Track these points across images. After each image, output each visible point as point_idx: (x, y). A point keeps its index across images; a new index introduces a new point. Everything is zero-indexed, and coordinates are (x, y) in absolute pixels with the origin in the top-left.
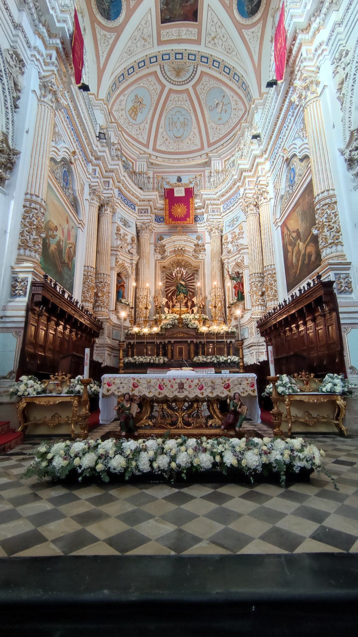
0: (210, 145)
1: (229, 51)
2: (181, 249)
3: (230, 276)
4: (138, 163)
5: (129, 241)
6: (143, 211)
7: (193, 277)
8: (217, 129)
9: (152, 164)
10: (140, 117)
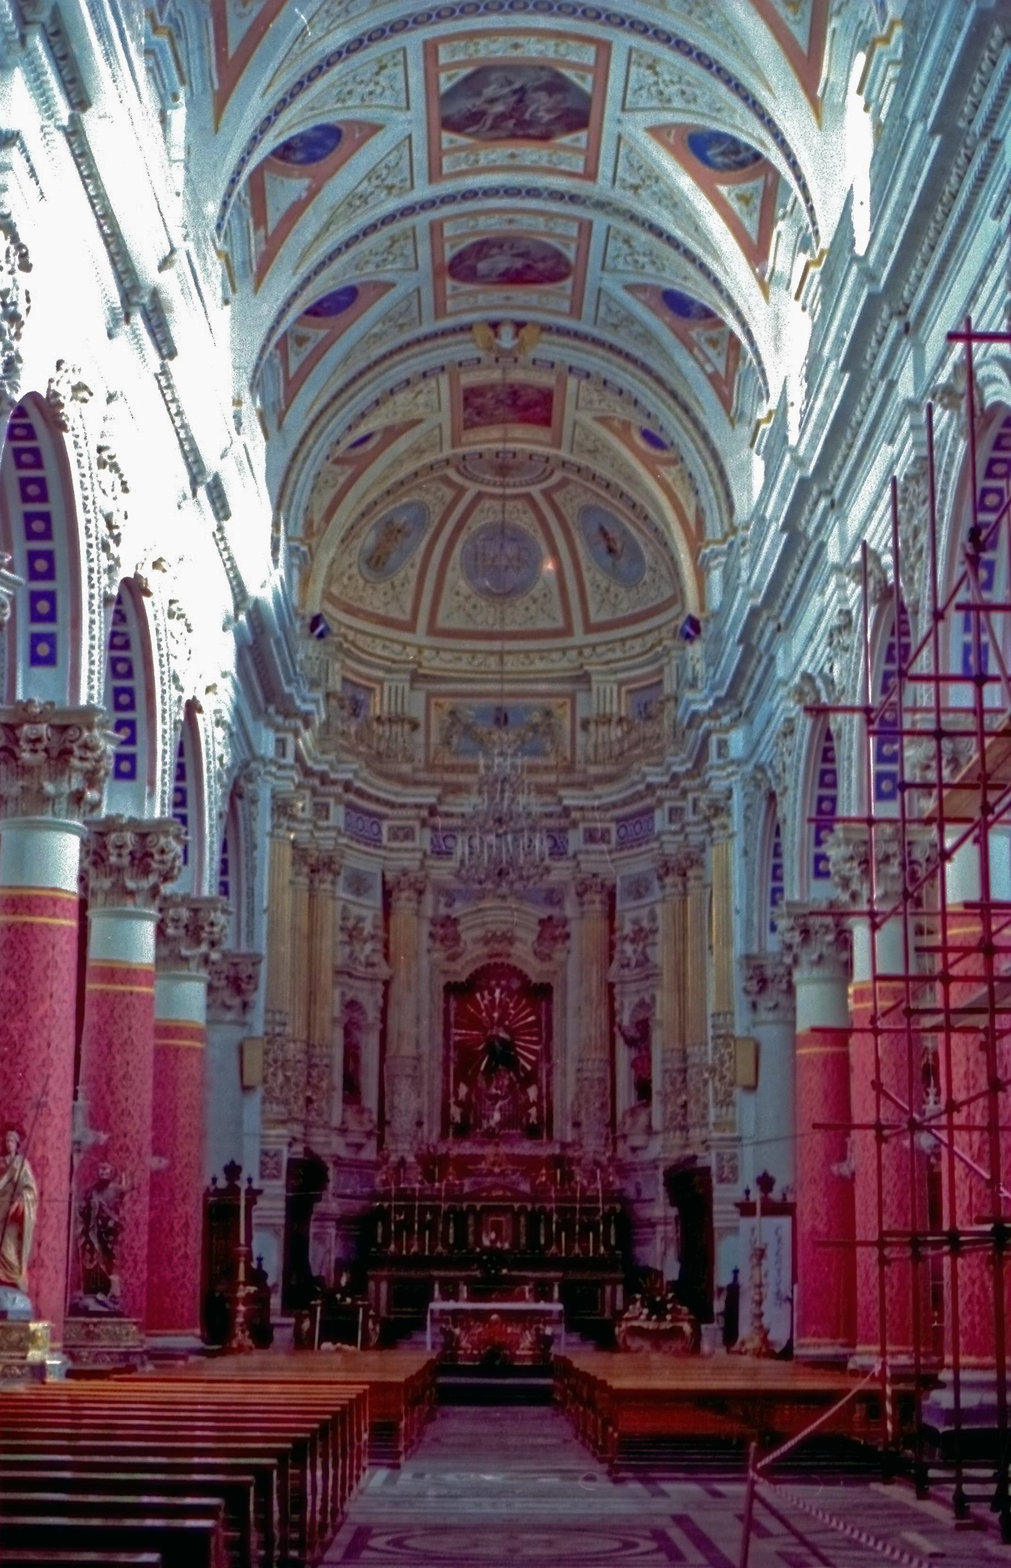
0: (590, 628)
1: (631, 478)
4: (386, 686)
6: (401, 834)
8: (608, 590)
9: (425, 676)
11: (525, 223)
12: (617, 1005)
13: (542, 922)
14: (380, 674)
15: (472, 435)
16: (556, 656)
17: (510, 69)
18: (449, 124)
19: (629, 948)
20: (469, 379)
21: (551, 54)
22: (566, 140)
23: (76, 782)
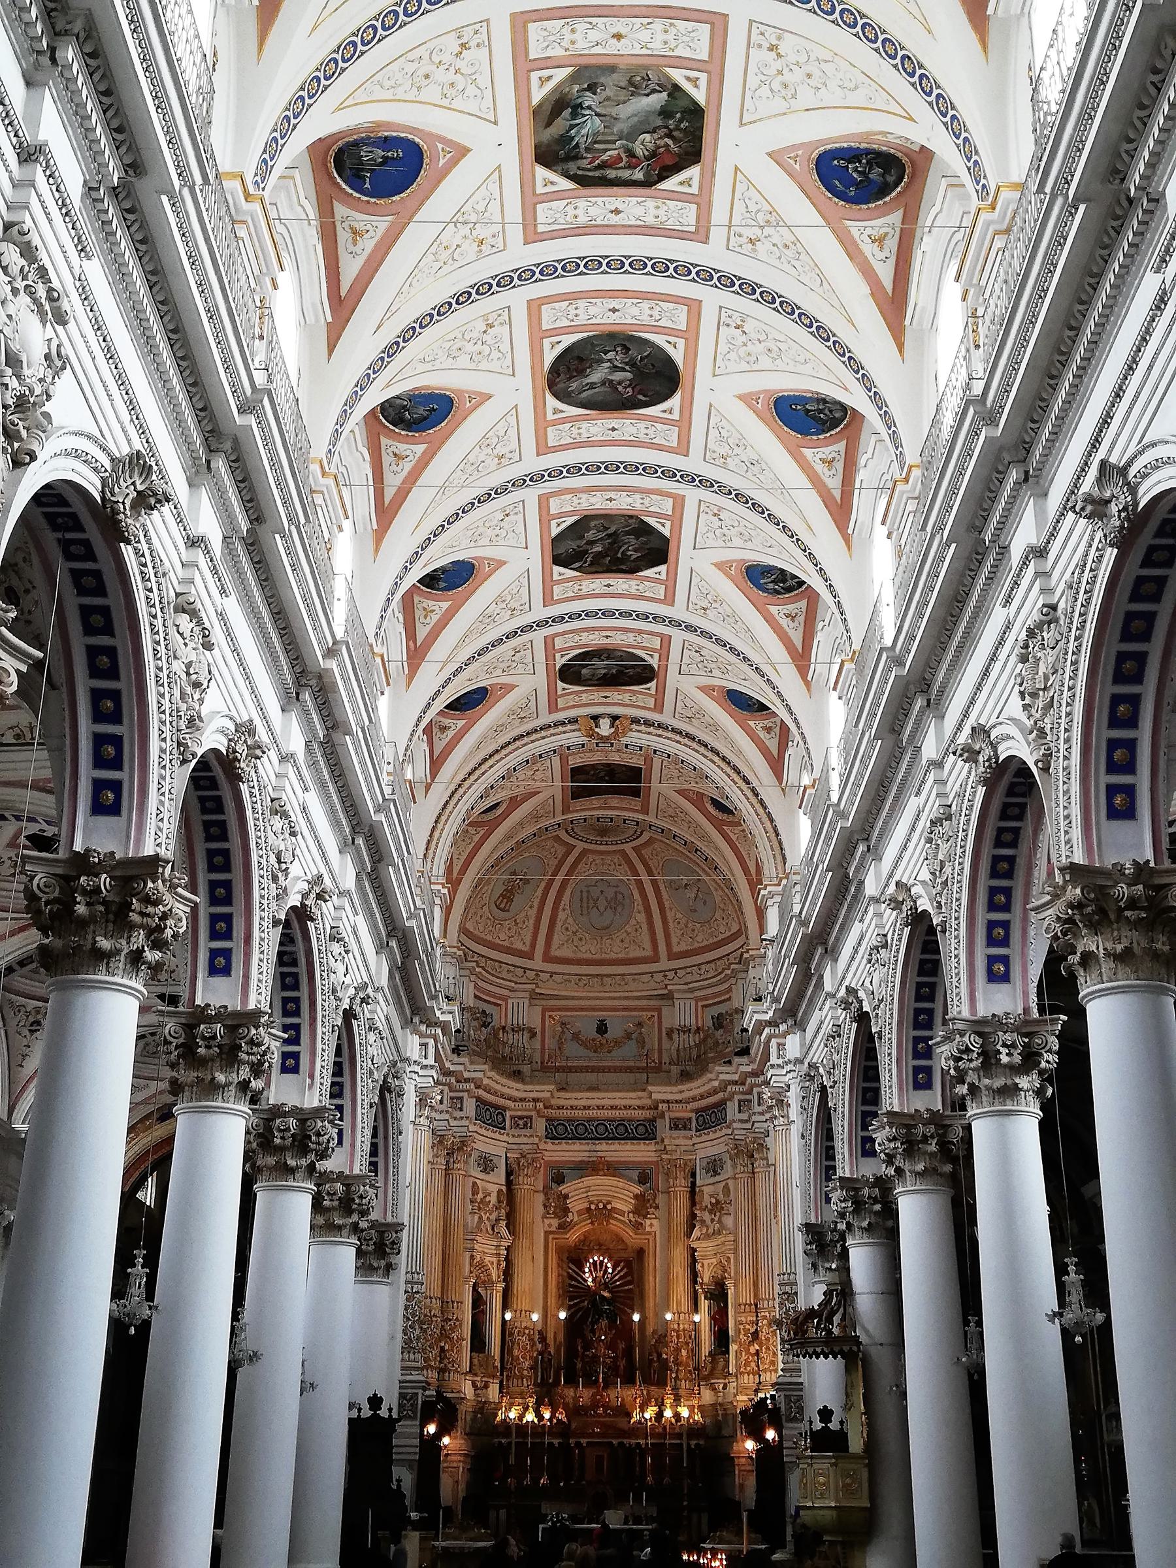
0: (672, 956)
1: (704, 837)
2: (605, 1206)
3: (705, 1293)
5: (493, 1199)
6: (521, 1122)
7: (629, 1278)
8: (686, 926)
10: (518, 899)
11: (618, 640)
12: (698, 1267)
13: (636, 1197)
14: (506, 992)
15: (578, 804)
16: (646, 978)
17: (608, 517)
18: (558, 560)
19: (707, 1217)
20: (575, 761)
21: (638, 506)
22: (650, 573)
23: (245, 1073)
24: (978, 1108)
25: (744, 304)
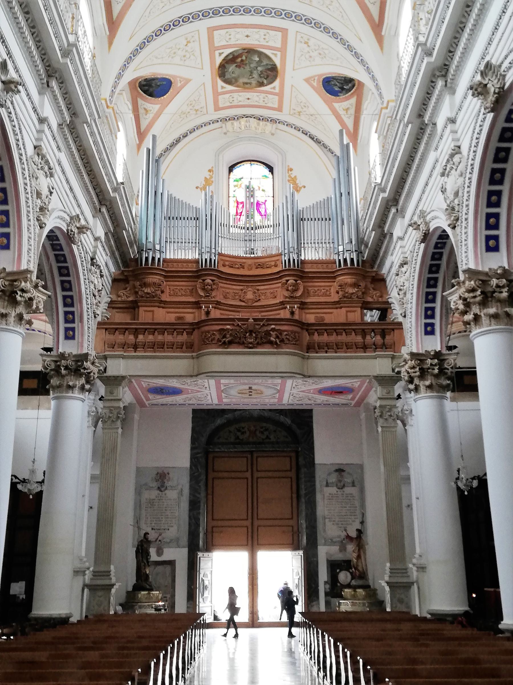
24: (479, 328)
25: (306, 29)
